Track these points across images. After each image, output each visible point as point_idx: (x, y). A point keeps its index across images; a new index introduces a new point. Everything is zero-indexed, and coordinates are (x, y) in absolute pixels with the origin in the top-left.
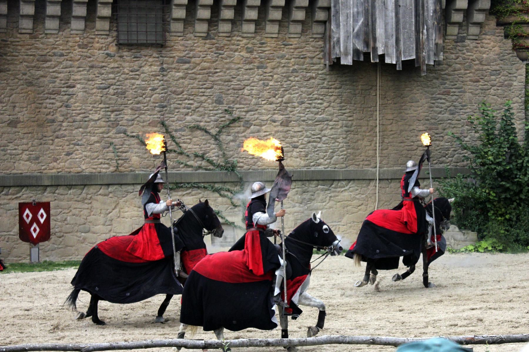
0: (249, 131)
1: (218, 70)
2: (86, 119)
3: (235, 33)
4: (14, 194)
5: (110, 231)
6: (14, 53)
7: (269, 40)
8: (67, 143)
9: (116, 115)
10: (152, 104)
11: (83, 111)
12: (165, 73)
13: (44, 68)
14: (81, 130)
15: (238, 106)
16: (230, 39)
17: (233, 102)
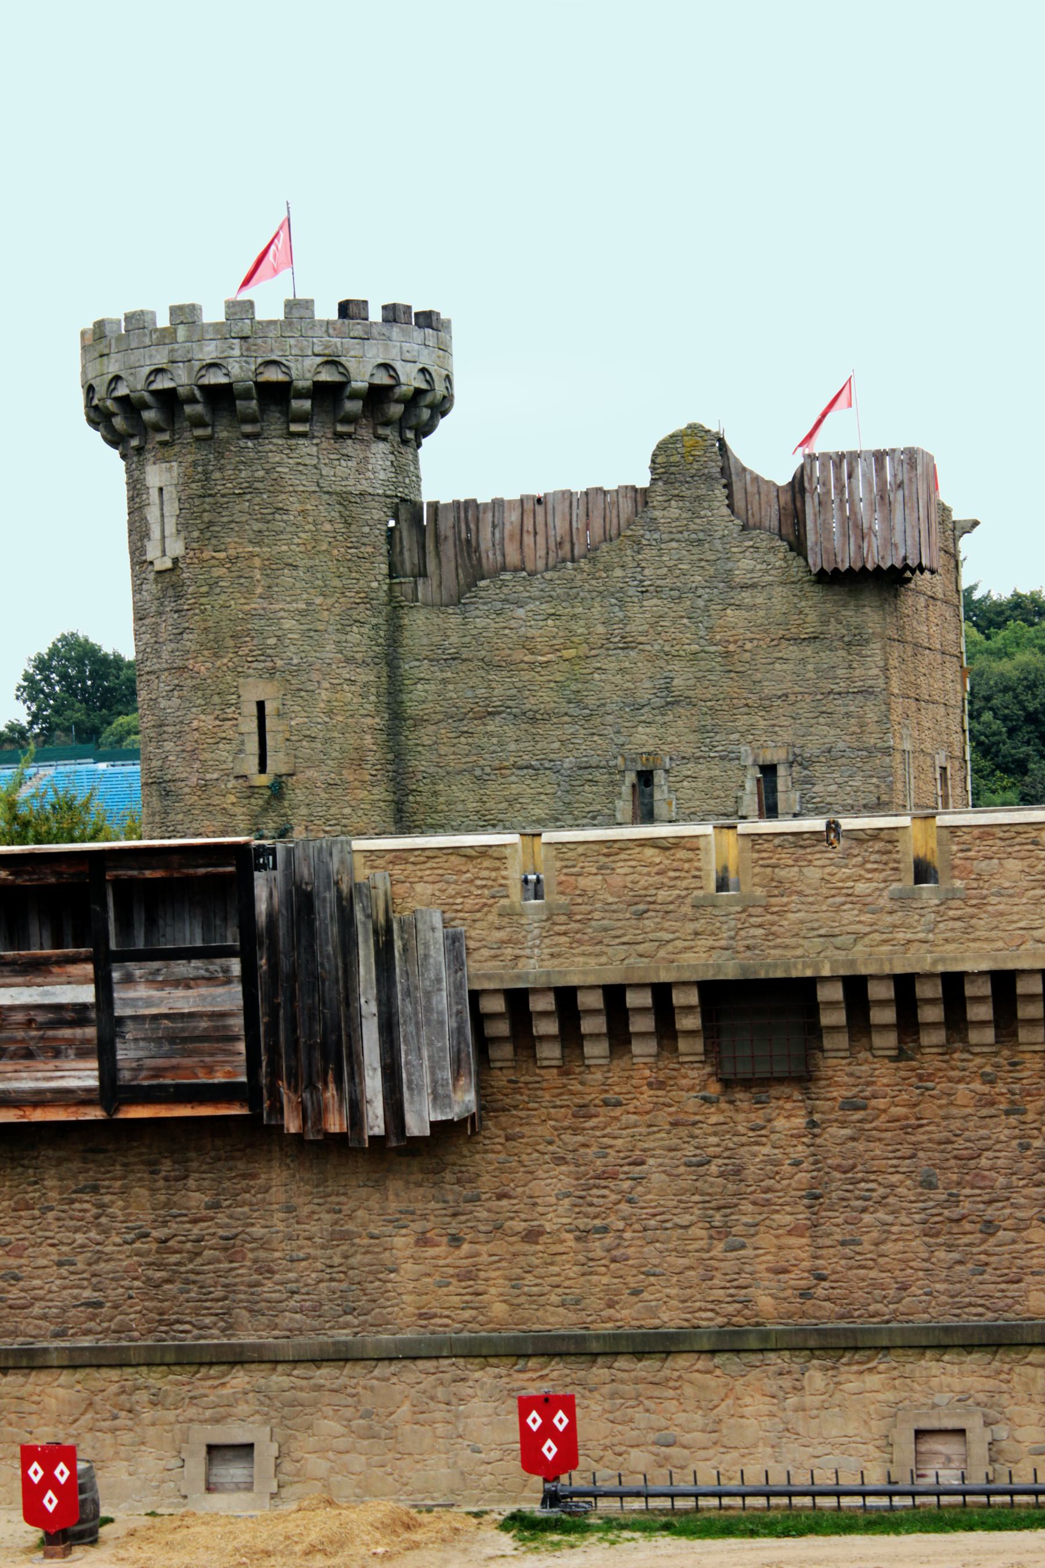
0: (992, 1241)
1: (924, 1122)
2: (668, 1225)
3: (956, 1045)
4: (535, 1370)
5: (715, 1443)
6: (531, 1105)
7: (1028, 1056)
8: (634, 1271)
9: (725, 1216)
10: (794, 1193)
11: (661, 1209)
12: (816, 1131)
13: (584, 1129)
14: (658, 1245)
15: (967, 1191)
16: (947, 1057)
17: (959, 1184)
